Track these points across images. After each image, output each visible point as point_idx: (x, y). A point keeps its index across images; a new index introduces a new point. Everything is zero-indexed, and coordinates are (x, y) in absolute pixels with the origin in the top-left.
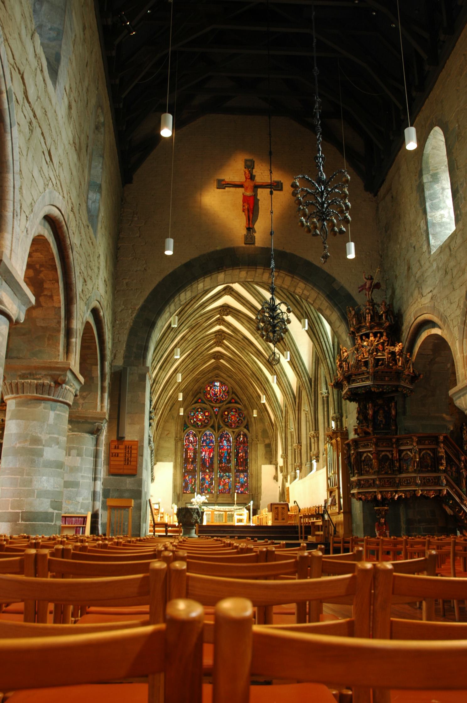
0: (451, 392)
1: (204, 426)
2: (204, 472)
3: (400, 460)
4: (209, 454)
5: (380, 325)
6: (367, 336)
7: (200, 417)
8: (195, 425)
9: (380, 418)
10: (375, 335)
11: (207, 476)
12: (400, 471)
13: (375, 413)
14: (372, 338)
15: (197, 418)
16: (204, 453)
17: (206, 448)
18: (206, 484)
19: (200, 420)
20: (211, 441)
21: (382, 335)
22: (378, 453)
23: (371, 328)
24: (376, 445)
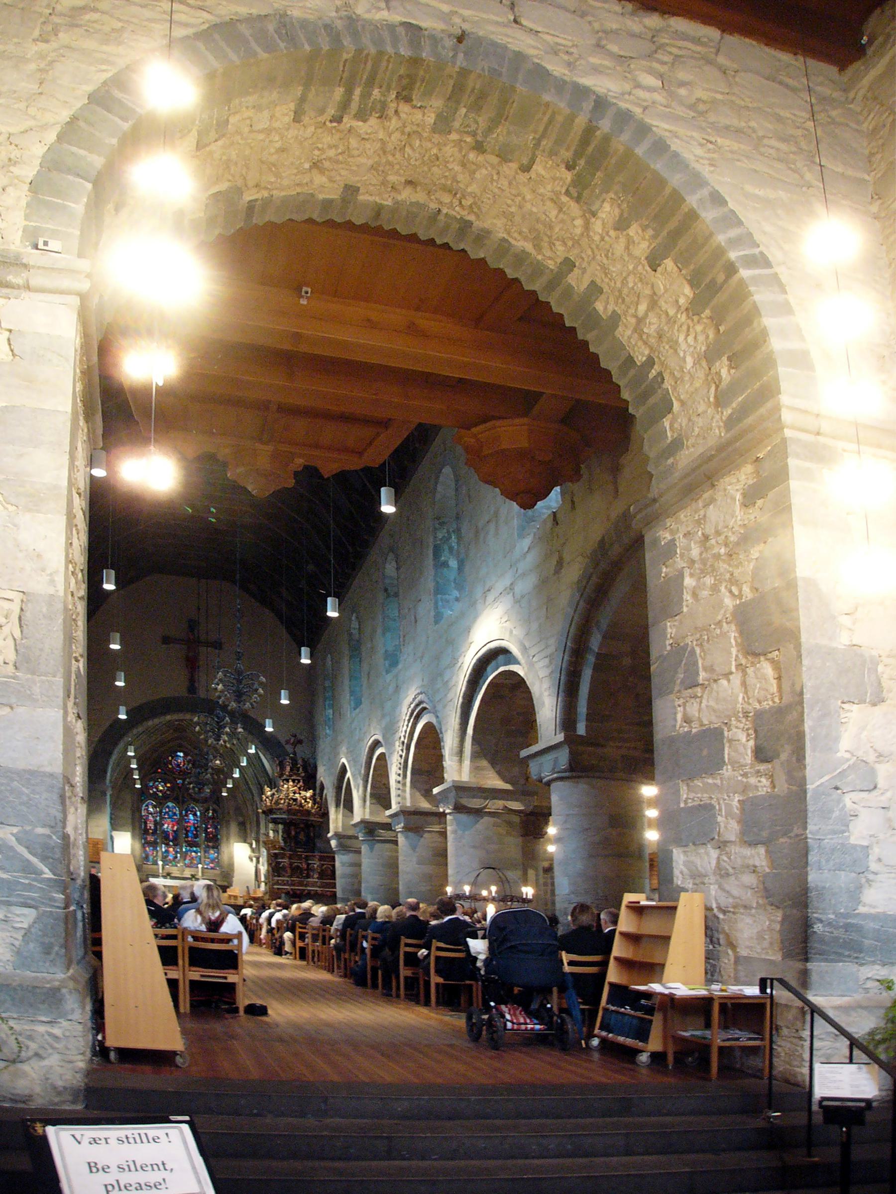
0: (329, 835)
1: (166, 798)
2: (167, 845)
3: (308, 869)
4: (173, 827)
5: (298, 775)
6: (288, 781)
7: (161, 788)
8: (154, 796)
9: (302, 836)
10: (293, 781)
11: (171, 849)
12: (308, 876)
13: (296, 833)
14: (291, 783)
15: (157, 788)
16: (166, 826)
17: (169, 820)
18: (171, 857)
19: (161, 791)
20: (175, 814)
21: (299, 782)
22: (291, 864)
23: (290, 776)
24: (290, 858)
